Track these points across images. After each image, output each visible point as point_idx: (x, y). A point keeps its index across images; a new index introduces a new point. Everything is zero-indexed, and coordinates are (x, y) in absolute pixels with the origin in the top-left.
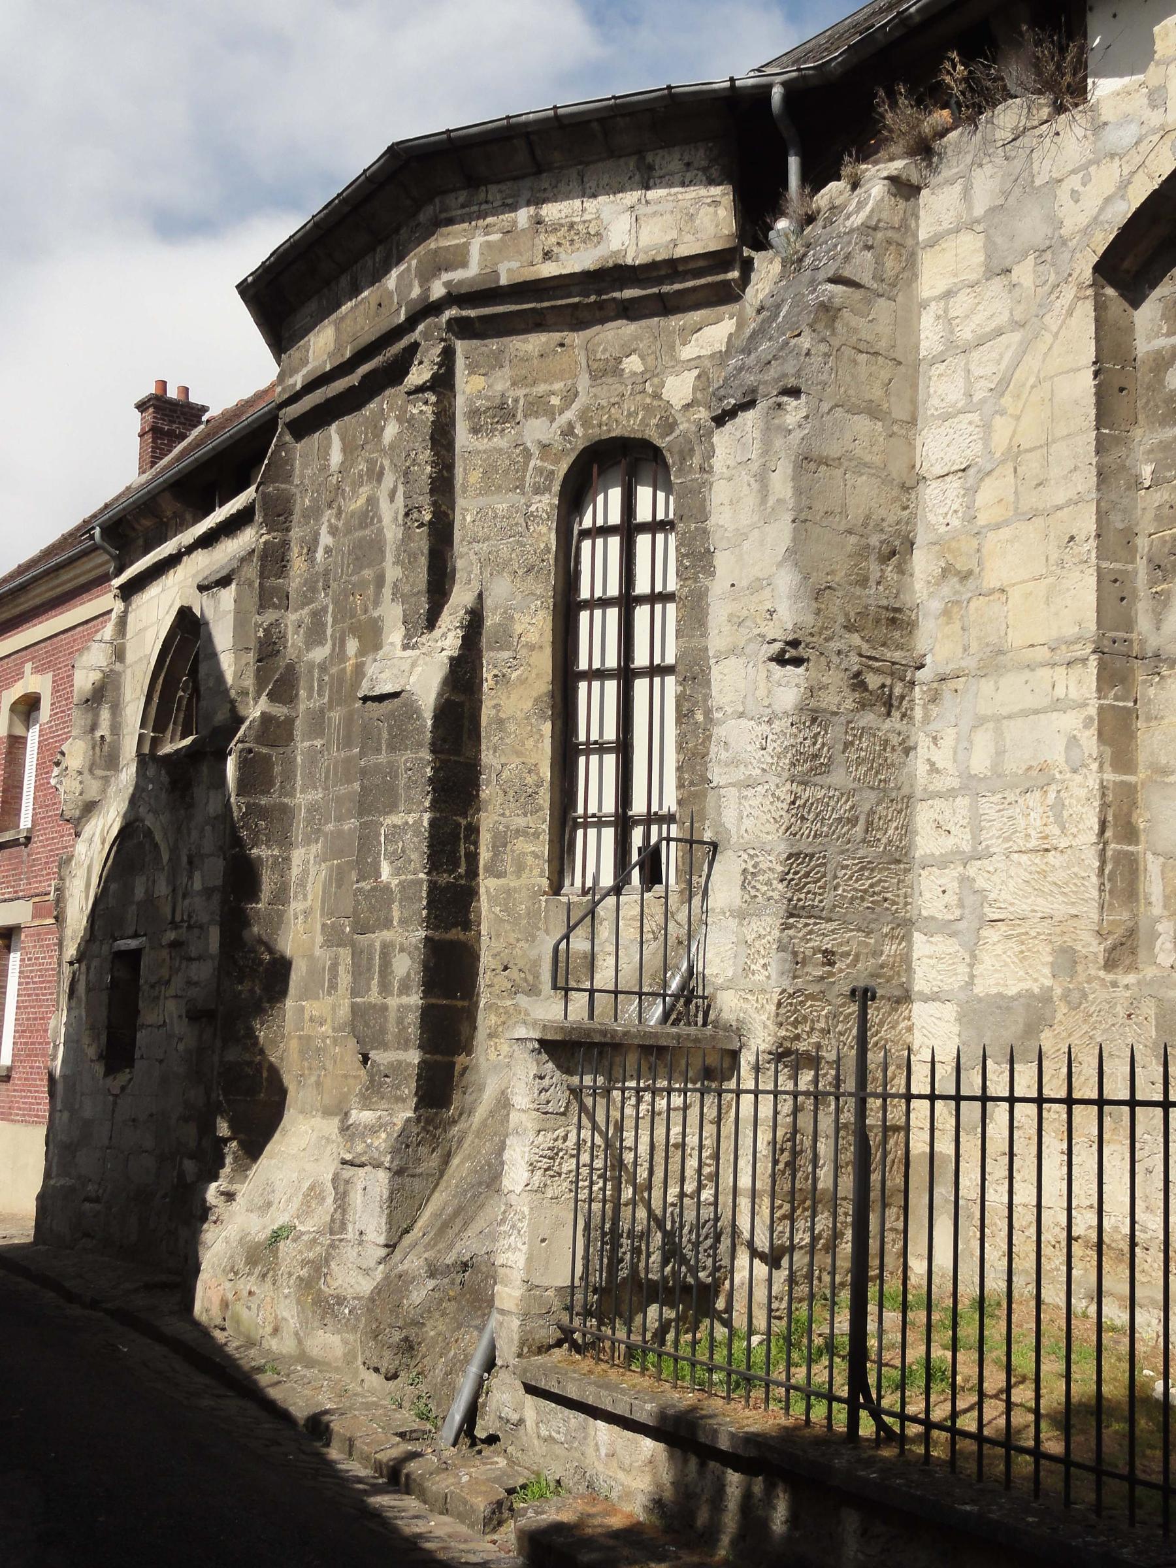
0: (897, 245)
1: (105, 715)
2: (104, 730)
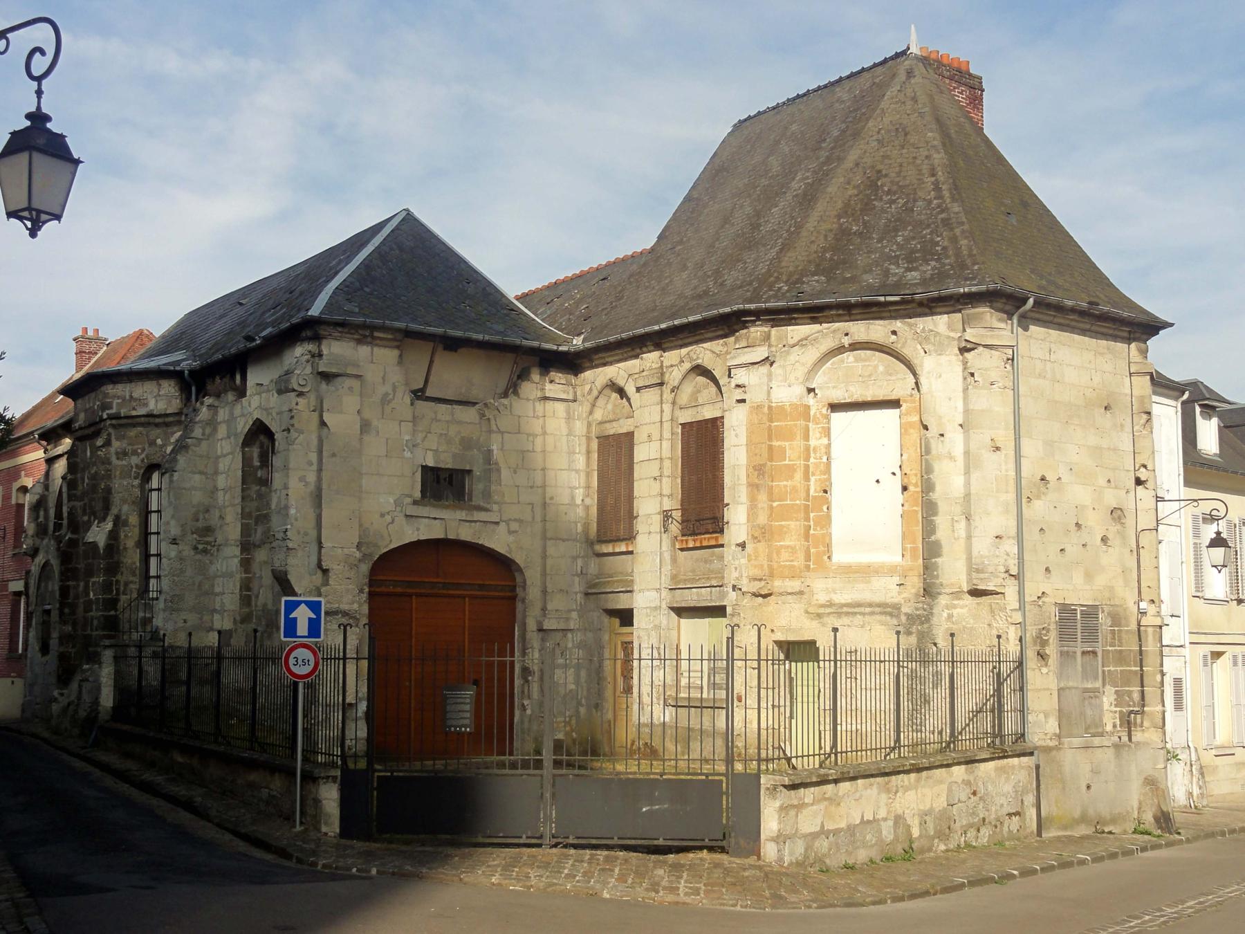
0: (212, 423)
1: (42, 513)
2: (41, 519)
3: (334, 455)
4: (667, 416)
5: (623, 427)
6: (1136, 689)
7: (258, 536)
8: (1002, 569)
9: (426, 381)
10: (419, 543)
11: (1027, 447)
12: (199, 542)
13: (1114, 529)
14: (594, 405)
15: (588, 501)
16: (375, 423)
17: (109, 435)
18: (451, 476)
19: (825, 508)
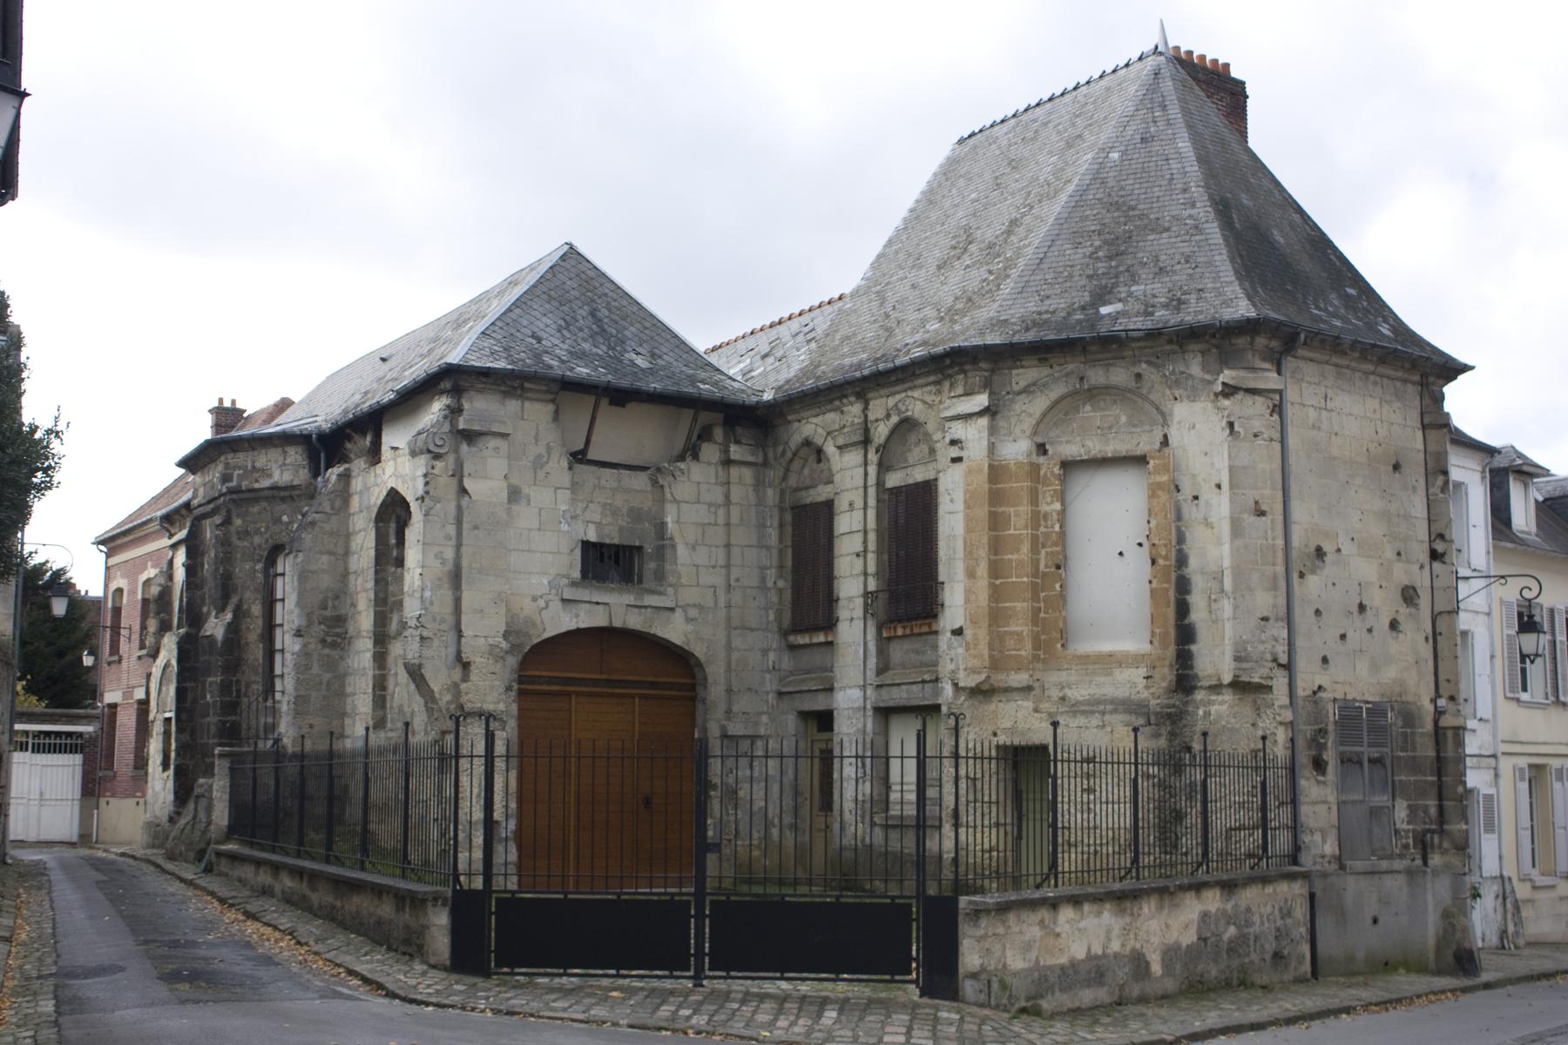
3: (476, 527)
4: (872, 480)
5: (821, 494)
6: (1432, 804)
7: (394, 626)
8: (1269, 657)
9: (588, 442)
10: (578, 631)
11: (1299, 513)
12: (327, 634)
13: (1404, 610)
14: (787, 470)
15: (781, 584)
16: (525, 490)
17: (229, 512)
18: (617, 553)
19: (1058, 586)
